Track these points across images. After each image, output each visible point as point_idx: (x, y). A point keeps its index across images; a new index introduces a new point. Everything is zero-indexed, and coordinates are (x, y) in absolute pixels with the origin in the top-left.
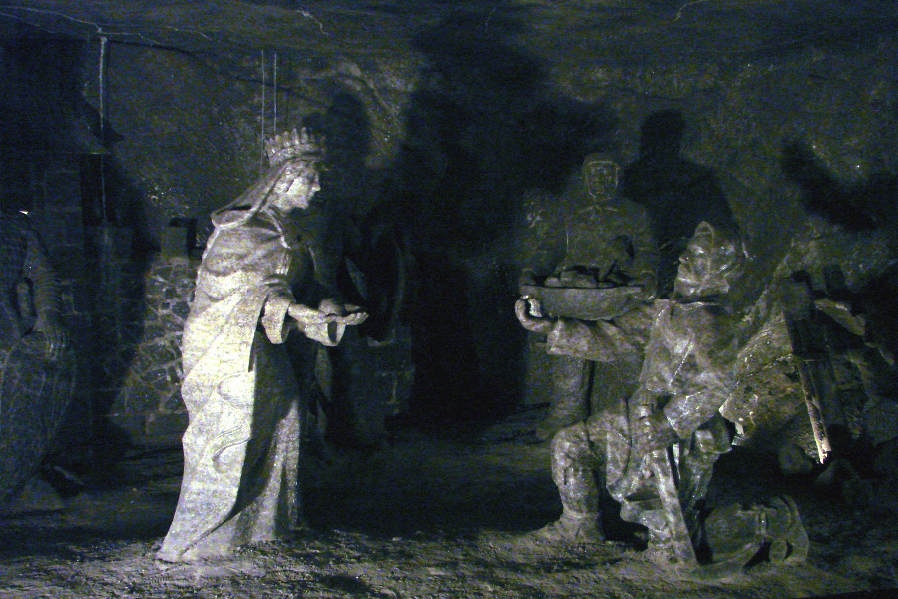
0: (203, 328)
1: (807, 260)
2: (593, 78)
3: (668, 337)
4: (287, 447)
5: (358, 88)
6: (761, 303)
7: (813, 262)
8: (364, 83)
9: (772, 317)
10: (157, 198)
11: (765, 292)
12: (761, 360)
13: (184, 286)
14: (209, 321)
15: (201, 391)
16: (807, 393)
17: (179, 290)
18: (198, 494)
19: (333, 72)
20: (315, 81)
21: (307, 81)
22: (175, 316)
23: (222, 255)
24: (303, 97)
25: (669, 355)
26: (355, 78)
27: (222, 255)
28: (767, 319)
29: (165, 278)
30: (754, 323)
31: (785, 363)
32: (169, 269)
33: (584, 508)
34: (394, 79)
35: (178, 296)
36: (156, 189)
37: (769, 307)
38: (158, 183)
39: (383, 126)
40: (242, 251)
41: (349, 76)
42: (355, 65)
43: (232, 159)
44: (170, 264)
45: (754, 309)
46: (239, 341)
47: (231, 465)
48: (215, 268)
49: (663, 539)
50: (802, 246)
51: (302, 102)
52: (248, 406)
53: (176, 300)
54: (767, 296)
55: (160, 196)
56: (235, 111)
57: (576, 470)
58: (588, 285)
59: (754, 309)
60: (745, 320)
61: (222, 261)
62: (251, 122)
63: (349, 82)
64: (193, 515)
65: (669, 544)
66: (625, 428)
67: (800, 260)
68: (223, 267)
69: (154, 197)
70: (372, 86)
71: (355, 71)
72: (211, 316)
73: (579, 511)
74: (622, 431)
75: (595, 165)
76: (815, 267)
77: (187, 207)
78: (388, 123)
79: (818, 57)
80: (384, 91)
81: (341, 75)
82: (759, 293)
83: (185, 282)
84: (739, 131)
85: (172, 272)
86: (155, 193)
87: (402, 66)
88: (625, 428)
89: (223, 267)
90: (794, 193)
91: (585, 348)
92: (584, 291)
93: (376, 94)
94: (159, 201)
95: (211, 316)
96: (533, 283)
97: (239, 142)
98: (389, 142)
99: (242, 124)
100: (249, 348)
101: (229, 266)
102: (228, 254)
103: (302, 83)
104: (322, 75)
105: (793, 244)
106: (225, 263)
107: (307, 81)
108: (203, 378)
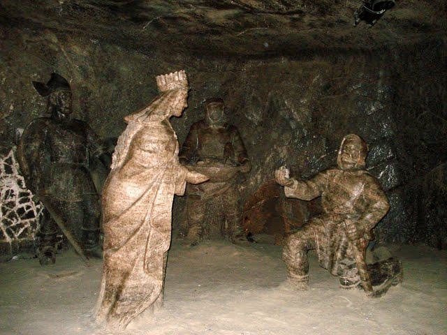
0: (135, 185)
3: (347, 188)
5: (57, 50)
8: (59, 47)
20: (31, 42)
26: (54, 43)
34: (75, 47)
46: (166, 192)
47: (156, 268)
48: (147, 149)
63: (51, 46)
65: (358, 284)
71: (55, 40)
73: (301, 275)
75: (214, 104)
79: (284, 61)
88: (324, 231)
93: (65, 55)
104: (34, 39)
105: (275, 148)
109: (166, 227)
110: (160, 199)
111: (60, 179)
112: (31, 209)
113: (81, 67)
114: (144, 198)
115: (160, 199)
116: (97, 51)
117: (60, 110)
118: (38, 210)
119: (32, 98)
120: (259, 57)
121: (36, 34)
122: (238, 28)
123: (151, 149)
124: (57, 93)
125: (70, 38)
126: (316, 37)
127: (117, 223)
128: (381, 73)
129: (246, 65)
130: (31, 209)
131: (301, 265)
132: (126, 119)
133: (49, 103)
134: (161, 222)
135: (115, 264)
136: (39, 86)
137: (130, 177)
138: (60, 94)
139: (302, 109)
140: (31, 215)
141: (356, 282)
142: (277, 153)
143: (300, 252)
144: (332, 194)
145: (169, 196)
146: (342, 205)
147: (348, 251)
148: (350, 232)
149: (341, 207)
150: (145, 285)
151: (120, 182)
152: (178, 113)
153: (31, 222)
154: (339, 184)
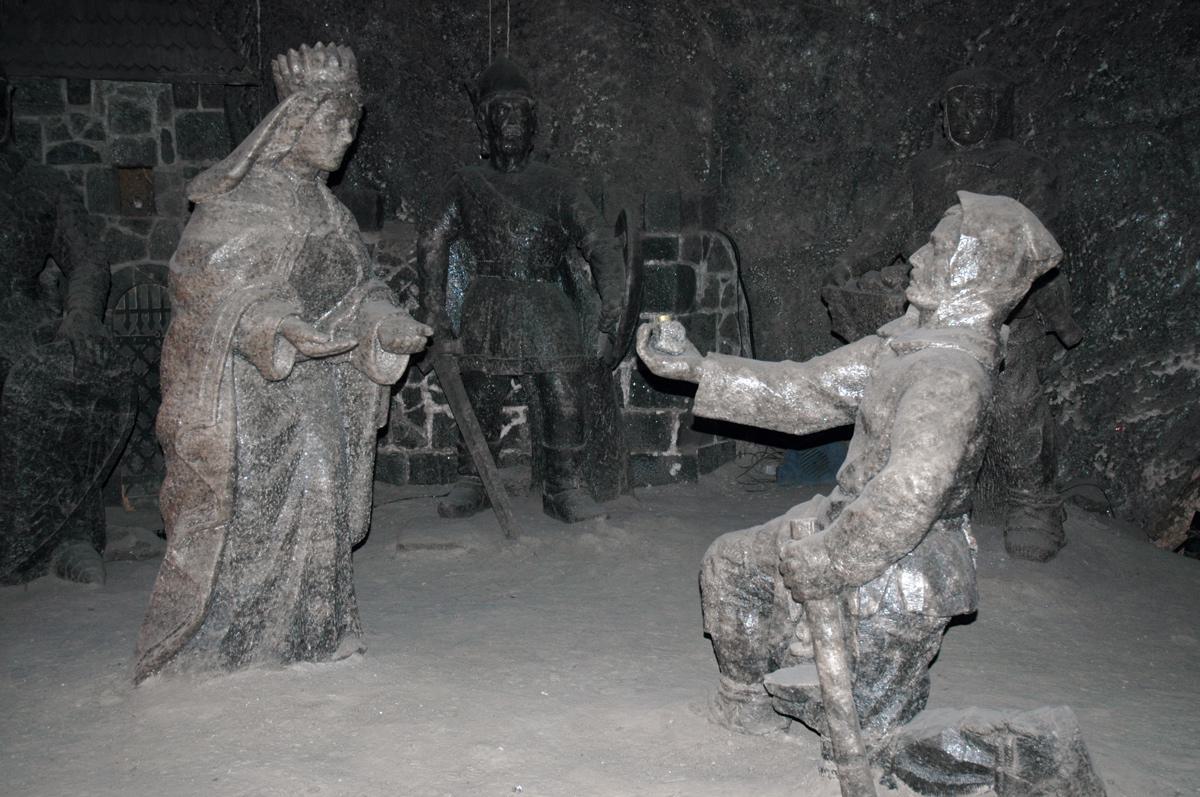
4: (314, 534)
119: (574, 114)
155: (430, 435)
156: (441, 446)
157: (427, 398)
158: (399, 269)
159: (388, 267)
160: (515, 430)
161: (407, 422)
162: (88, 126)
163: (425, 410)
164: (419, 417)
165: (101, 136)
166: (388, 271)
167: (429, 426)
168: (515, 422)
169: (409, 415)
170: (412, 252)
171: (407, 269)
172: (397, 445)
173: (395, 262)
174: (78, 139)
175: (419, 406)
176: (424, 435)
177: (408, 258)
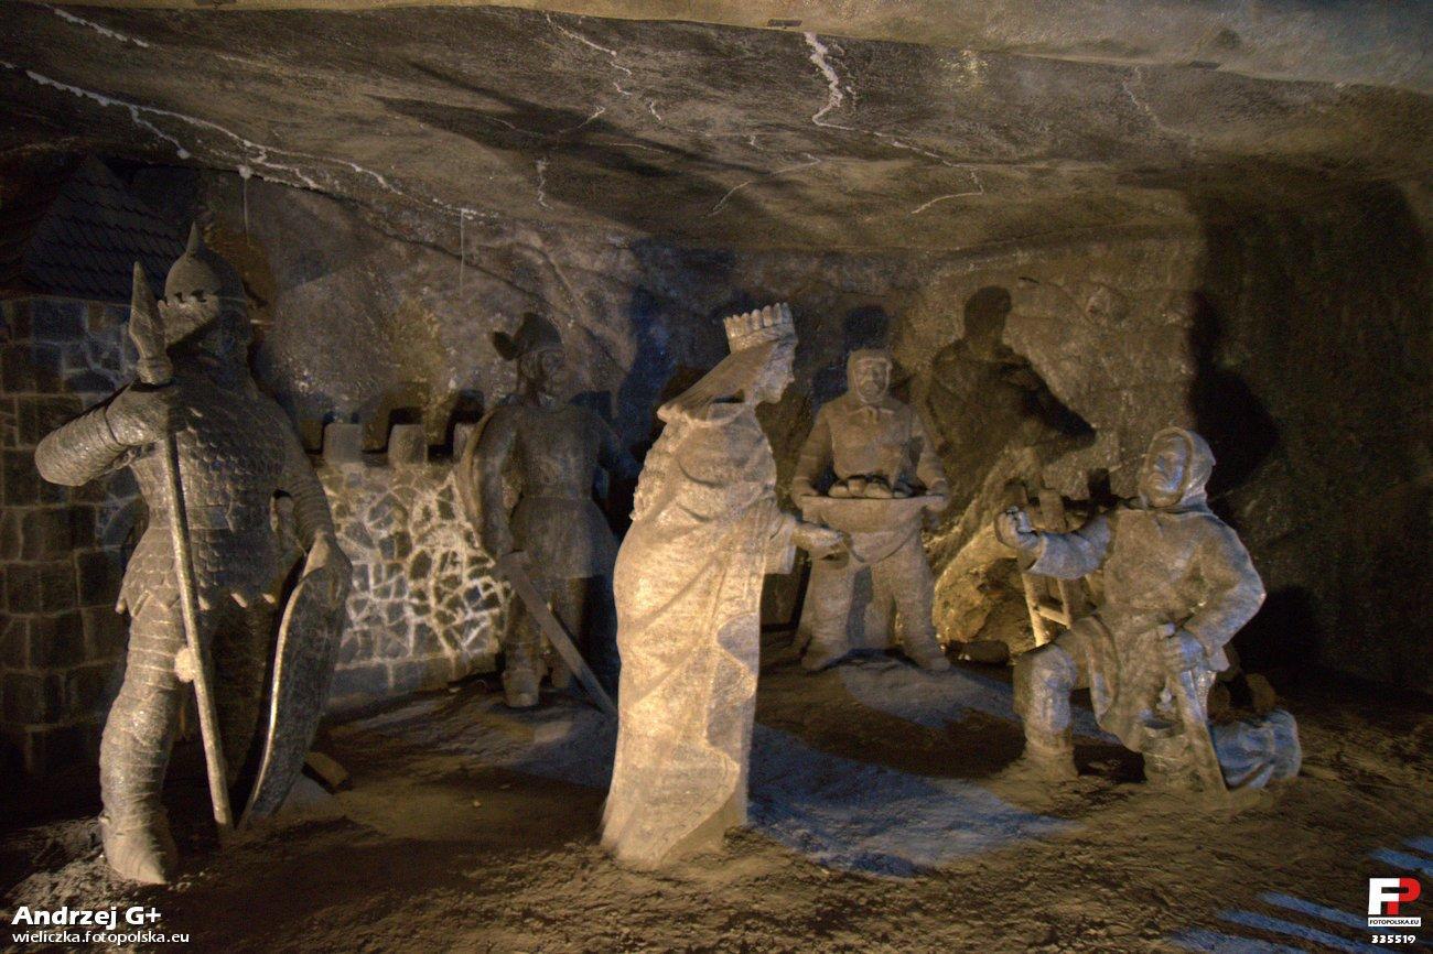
1: (1021, 467)
2: (786, 268)
6: (970, 512)
7: (1028, 469)
8: (545, 256)
9: (982, 527)
10: (306, 385)
11: (974, 502)
12: (956, 573)
13: (360, 501)
14: (691, 547)
15: (675, 640)
16: (1034, 604)
17: (354, 507)
18: (679, 777)
19: (509, 241)
20: (488, 249)
21: (479, 248)
22: (349, 540)
23: (713, 461)
24: (476, 267)
25: (1166, 570)
26: (533, 249)
27: (713, 461)
28: (976, 529)
29: (336, 490)
30: (962, 534)
31: (977, 574)
32: (340, 480)
33: (1061, 742)
35: (353, 514)
36: (305, 374)
37: (979, 515)
38: (308, 366)
39: (566, 309)
40: (738, 456)
41: (528, 247)
42: (535, 234)
43: (391, 339)
44: (341, 472)
45: (962, 519)
46: (747, 572)
49: (1179, 767)
50: (1016, 453)
51: (477, 273)
52: (753, 654)
53: (352, 520)
54: (977, 506)
55: (310, 383)
56: (394, 279)
57: (1055, 701)
58: (885, 495)
59: (962, 519)
60: (953, 531)
61: (714, 467)
62: (414, 293)
63: (528, 254)
64: (672, 806)
65: (1188, 772)
66: (1111, 650)
67: (1013, 467)
68: (717, 476)
69: (303, 384)
70: (552, 261)
71: (536, 241)
72: (697, 541)
73: (1057, 746)
74: (1108, 654)
76: (1029, 474)
77: (347, 399)
78: (572, 305)
80: (566, 267)
81: (519, 244)
82: (968, 502)
83: (362, 496)
84: (940, 331)
85: (344, 483)
86: (304, 379)
87: (588, 239)
88: (1111, 650)
89: (717, 476)
90: (1004, 399)
91: (1061, 566)
92: (880, 502)
93: (558, 271)
94: (310, 389)
95: (697, 541)
96: (814, 493)
97: (398, 318)
98: (573, 328)
99: (403, 296)
100: (761, 581)
101: (726, 475)
102: (722, 459)
103: (474, 250)
104: (497, 243)
105: (1006, 451)
106: (719, 471)
107: (479, 248)
108: (682, 622)
109: (745, 649)
110: (731, 588)
111: (545, 531)
112: (492, 590)
113: (590, 295)
114: (699, 585)
115: (731, 588)
116: (623, 260)
117: (543, 390)
118: (506, 592)
120: (968, 254)
121: (499, 233)
122: (919, 196)
123: (712, 478)
124: (535, 354)
125: (566, 239)
126: (1090, 206)
127: (641, 636)
128: (1247, 280)
129: (939, 274)
130: (492, 590)
131: (1054, 724)
132: (662, 413)
133: (521, 373)
134: (737, 634)
135: (642, 723)
136: (500, 340)
137: (669, 541)
138: (541, 356)
139: (1067, 365)
140: (492, 602)
141: (1186, 767)
142: (1012, 462)
143: (1053, 697)
144: (1127, 565)
145: (754, 580)
146: (1151, 590)
147: (1165, 697)
148: (1169, 654)
149: (1149, 595)
150: (704, 770)
151: (648, 550)
152: (777, 394)
153: (493, 617)
154: (1144, 541)
155: (411, 645)
156: (421, 653)
157: (409, 612)
158: (383, 495)
159: (375, 494)
160: (484, 632)
161: (390, 635)
162: (105, 355)
163: (407, 622)
164: (401, 629)
165: (117, 366)
166: (374, 498)
167: (411, 637)
168: (483, 625)
169: (394, 629)
170: (395, 480)
171: (389, 496)
172: (382, 656)
173: (380, 489)
174: (97, 367)
175: (401, 619)
176: (405, 645)
177: (391, 486)
